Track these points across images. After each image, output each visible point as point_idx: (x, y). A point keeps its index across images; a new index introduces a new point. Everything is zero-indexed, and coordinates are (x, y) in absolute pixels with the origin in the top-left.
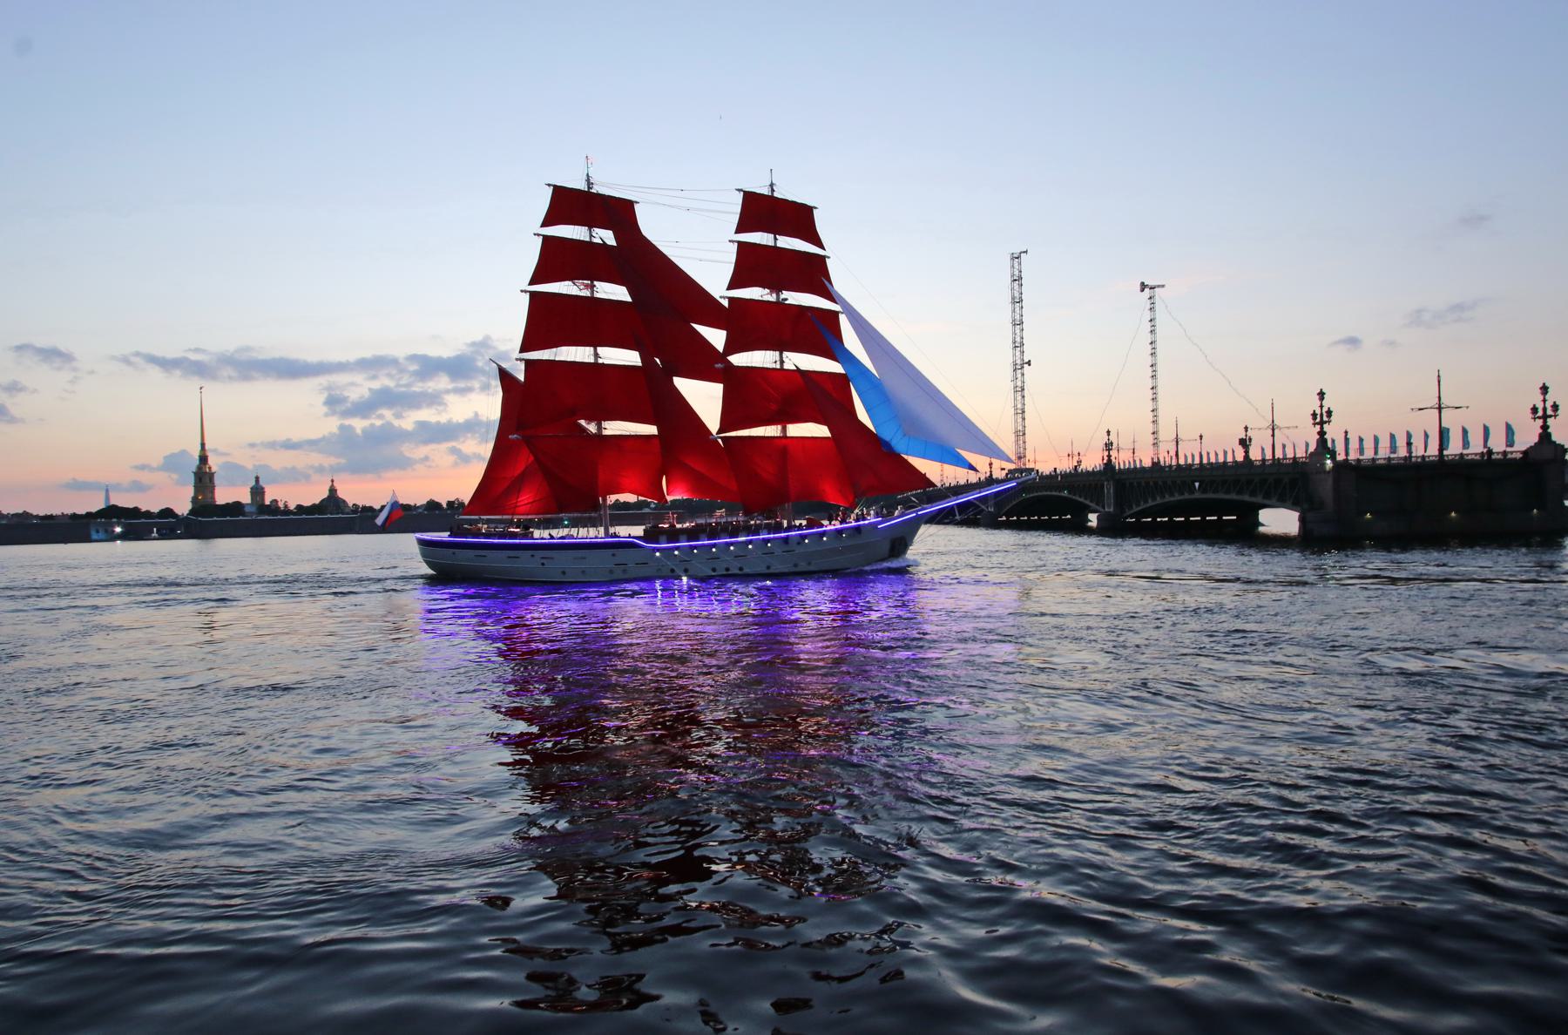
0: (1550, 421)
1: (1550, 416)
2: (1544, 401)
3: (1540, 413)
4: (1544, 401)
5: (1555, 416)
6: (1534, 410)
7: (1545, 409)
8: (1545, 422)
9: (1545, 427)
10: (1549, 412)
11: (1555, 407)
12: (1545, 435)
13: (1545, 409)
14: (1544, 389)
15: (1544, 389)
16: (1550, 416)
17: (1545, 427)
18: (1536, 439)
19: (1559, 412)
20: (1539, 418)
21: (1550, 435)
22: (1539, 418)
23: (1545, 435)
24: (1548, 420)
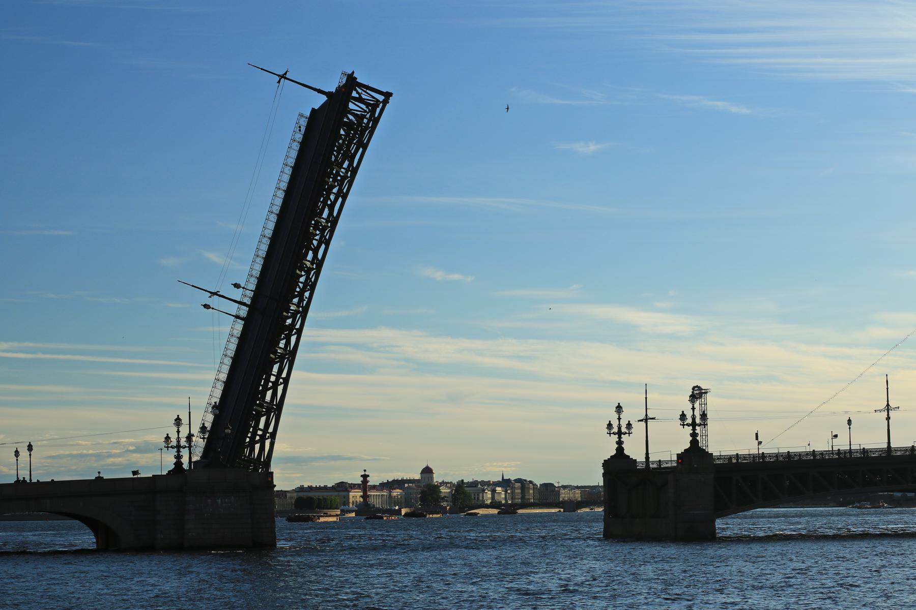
0: (624, 438)
1: (626, 433)
2: (619, 419)
3: (615, 430)
4: (619, 419)
5: (629, 433)
6: (610, 426)
7: (619, 427)
8: (620, 437)
9: (620, 443)
10: (624, 430)
11: (629, 425)
12: (620, 449)
13: (619, 427)
14: (619, 408)
15: (619, 408)
16: (626, 433)
17: (620, 443)
18: (614, 452)
19: (632, 430)
20: (614, 433)
21: (623, 449)
22: (613, 433)
23: (620, 449)
24: (622, 436)
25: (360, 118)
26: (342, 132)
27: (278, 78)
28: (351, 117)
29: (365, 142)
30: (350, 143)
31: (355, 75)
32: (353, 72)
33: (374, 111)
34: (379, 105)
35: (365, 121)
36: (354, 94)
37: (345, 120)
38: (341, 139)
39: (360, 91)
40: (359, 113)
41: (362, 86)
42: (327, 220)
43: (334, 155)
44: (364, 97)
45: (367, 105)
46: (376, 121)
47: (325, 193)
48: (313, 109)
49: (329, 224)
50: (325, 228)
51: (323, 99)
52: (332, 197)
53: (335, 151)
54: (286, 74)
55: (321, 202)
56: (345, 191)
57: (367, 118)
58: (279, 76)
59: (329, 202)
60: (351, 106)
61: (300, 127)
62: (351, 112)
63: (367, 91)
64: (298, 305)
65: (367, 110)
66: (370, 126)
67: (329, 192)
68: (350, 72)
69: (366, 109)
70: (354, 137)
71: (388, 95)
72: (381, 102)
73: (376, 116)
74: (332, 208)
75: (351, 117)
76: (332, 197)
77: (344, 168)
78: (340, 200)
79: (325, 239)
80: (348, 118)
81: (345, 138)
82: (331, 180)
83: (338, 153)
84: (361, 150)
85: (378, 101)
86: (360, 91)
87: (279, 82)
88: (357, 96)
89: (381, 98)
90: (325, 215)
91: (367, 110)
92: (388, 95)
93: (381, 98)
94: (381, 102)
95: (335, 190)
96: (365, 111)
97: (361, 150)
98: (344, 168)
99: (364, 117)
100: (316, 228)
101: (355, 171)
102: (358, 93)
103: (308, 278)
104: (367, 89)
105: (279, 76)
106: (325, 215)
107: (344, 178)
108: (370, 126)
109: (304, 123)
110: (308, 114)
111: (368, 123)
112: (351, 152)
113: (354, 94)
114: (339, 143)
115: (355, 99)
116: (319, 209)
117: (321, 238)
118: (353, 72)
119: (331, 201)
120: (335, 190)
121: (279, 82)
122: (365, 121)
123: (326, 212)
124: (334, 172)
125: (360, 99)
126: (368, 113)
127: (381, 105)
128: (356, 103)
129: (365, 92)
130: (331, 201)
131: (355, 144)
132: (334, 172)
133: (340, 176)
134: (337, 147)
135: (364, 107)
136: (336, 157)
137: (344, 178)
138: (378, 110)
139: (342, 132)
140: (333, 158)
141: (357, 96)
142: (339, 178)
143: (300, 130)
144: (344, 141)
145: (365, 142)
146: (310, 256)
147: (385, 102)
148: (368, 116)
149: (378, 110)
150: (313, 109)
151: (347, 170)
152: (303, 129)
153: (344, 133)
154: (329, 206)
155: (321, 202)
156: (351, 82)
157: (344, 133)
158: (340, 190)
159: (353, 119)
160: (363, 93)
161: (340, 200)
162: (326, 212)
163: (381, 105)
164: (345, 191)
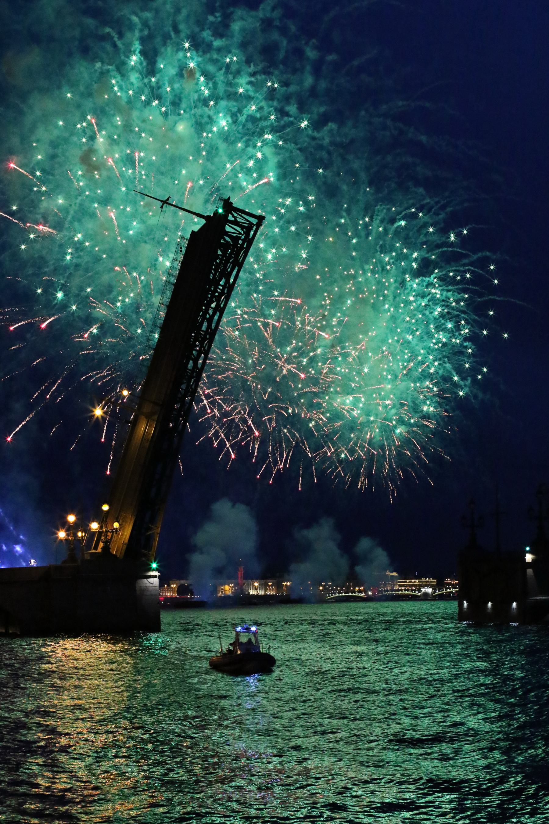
25: (235, 239)
26: (219, 252)
27: (160, 204)
28: (227, 239)
29: (240, 261)
30: (227, 261)
31: (231, 200)
32: (229, 198)
33: (247, 234)
34: (253, 227)
35: (240, 242)
36: (230, 217)
37: (222, 241)
38: (219, 258)
39: (235, 215)
40: (234, 235)
41: (237, 210)
42: (206, 332)
43: (212, 273)
44: (239, 220)
45: (242, 227)
46: (250, 242)
47: (204, 308)
48: (193, 232)
49: (208, 336)
50: (205, 339)
51: (203, 221)
52: (211, 311)
53: (213, 269)
54: (168, 199)
55: (201, 316)
56: (222, 306)
57: (242, 240)
58: (162, 201)
59: (208, 316)
60: (228, 229)
61: (181, 248)
62: (227, 234)
63: (243, 215)
64: (180, 410)
65: (242, 233)
66: (245, 246)
67: (208, 306)
68: (226, 198)
69: (241, 231)
70: (230, 257)
71: (261, 219)
72: (254, 225)
73: (250, 237)
74: (210, 321)
75: (227, 239)
76: (211, 311)
77: (221, 285)
78: (218, 314)
79: (204, 349)
80: (225, 240)
81: (223, 257)
82: (209, 296)
83: (216, 271)
84: (237, 268)
85: (251, 224)
86: (235, 215)
87: (162, 207)
88: (233, 219)
89: (254, 221)
90: (204, 328)
91: (242, 233)
92: (261, 219)
93: (254, 221)
94: (254, 225)
95: (213, 305)
96: (240, 233)
97: (237, 268)
98: (221, 285)
99: (239, 238)
100: (196, 339)
101: (230, 288)
102: (233, 216)
103: (188, 386)
104: (242, 213)
105: (162, 201)
106: (204, 328)
107: (221, 294)
108: (245, 246)
109: (185, 243)
110: (188, 236)
111: (243, 244)
112: (227, 271)
113: (230, 217)
114: (216, 262)
115: (231, 222)
116: (198, 322)
117: (200, 349)
118: (229, 198)
119: (209, 315)
120: (213, 305)
121: (162, 207)
122: (240, 242)
123: (205, 325)
124: (212, 289)
125: (236, 223)
126: (243, 235)
127: (255, 228)
128: (232, 225)
129: (240, 215)
130: (209, 315)
131: (231, 263)
132: (212, 289)
133: (217, 292)
134: (214, 265)
135: (239, 229)
136: (214, 275)
137: (221, 294)
138: (252, 233)
139: (219, 252)
140: (211, 276)
141: (233, 219)
142: (217, 294)
143: (181, 251)
144: (221, 260)
145: (240, 261)
146: (190, 365)
147: (259, 225)
148: (243, 237)
149: (252, 233)
150: (193, 232)
151: (224, 287)
152: (184, 249)
153: (221, 253)
154: (208, 319)
155: (201, 316)
156: (228, 205)
157: (221, 253)
158: (218, 305)
159: (230, 240)
160: (238, 216)
161: (218, 314)
162: (205, 325)
163: (255, 228)
164: (222, 306)
